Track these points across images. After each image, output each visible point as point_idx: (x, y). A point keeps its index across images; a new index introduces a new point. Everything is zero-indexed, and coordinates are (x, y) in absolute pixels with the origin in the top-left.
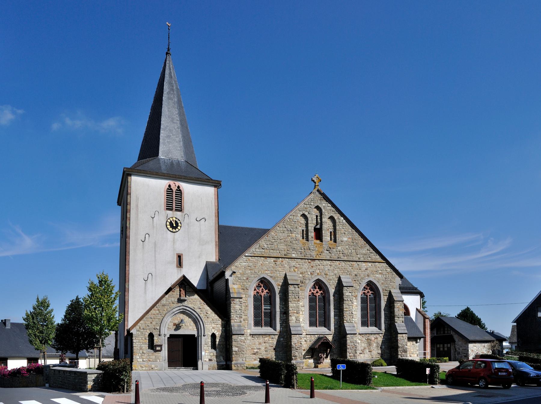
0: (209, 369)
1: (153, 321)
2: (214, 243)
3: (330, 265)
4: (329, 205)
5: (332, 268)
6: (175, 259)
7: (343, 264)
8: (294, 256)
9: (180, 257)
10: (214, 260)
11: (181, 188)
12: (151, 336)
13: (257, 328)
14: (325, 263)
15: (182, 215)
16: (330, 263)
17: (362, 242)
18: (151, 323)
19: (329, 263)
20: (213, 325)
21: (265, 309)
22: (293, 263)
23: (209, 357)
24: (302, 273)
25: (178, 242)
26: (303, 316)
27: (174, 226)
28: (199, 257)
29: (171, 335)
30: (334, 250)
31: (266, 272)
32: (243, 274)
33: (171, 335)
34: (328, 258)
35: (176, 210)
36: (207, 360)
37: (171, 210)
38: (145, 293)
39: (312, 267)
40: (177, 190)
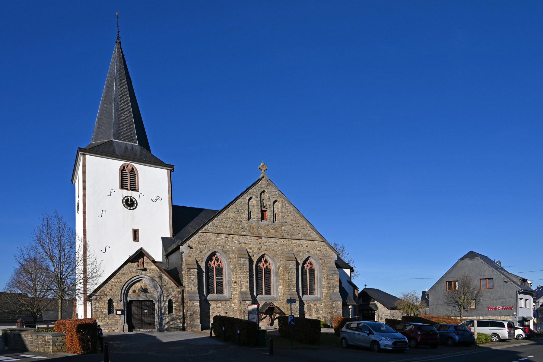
7: (286, 241)
8: (242, 233)
10: (169, 237)
14: (270, 240)
17: (302, 223)
19: (273, 240)
22: (242, 239)
27: (130, 203)
34: (274, 236)
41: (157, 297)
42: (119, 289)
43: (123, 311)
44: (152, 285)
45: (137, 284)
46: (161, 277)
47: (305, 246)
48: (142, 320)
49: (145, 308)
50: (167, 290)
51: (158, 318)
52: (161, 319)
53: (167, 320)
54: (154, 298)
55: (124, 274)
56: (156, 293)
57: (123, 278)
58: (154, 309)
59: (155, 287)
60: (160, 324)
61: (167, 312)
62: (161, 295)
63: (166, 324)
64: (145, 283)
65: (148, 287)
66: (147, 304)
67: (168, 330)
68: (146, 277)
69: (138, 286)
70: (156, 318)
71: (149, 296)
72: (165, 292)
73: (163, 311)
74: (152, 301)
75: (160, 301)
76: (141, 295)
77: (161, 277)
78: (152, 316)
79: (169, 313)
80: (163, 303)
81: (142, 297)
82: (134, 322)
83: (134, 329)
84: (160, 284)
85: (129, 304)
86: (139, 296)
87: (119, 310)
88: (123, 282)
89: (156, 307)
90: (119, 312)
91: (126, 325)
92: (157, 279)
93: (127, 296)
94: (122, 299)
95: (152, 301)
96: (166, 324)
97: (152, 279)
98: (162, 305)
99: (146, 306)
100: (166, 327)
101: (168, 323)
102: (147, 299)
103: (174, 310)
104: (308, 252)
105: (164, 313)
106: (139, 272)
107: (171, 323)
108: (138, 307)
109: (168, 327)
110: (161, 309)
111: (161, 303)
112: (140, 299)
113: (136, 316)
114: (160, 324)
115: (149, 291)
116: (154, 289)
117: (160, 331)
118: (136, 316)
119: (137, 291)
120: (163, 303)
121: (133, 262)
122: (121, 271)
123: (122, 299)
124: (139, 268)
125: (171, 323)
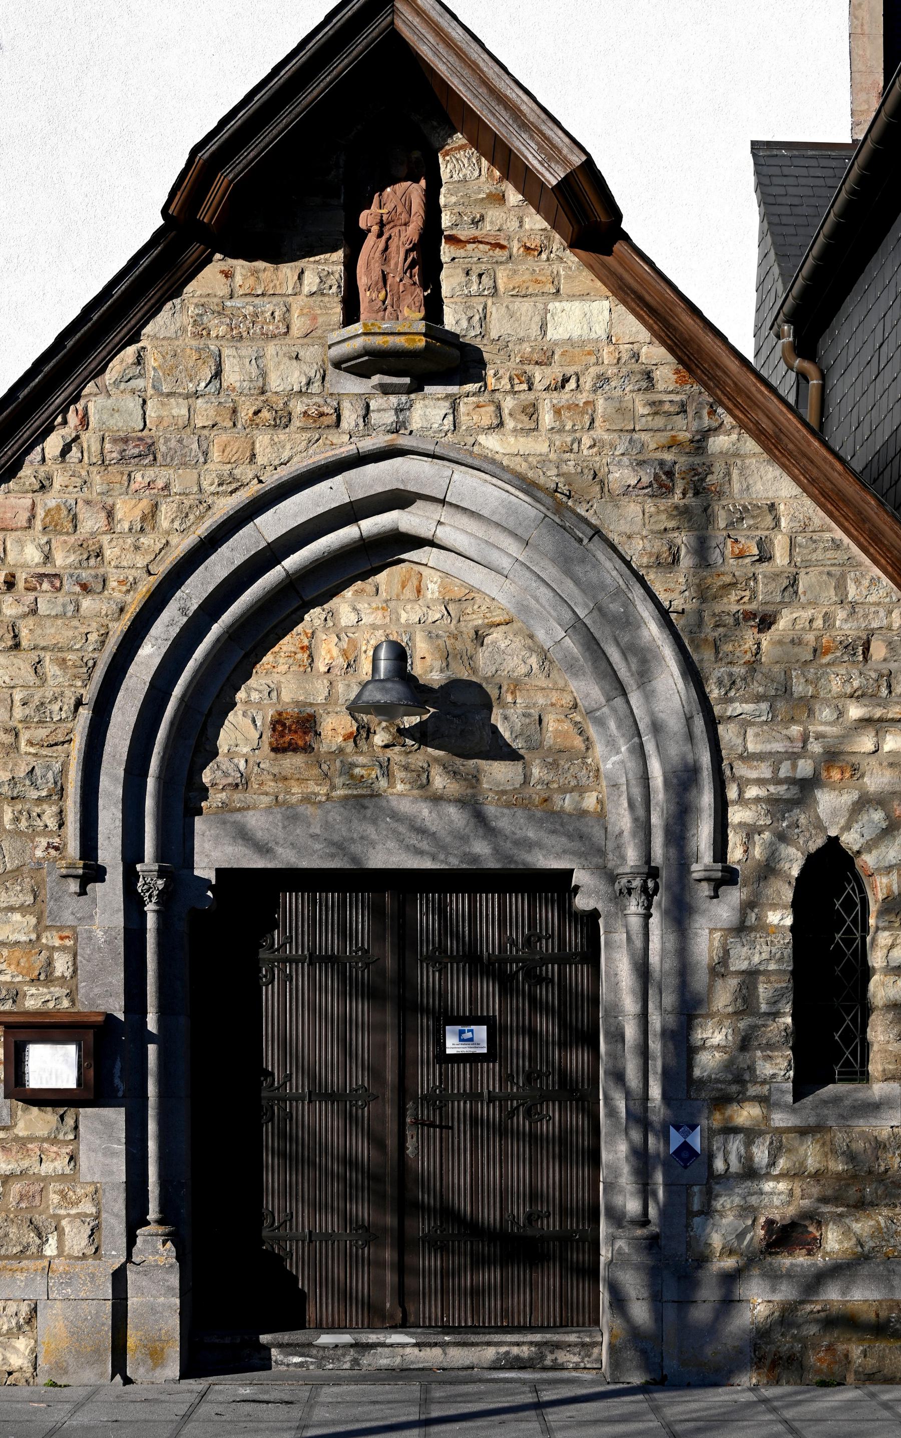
41: (622, 820)
42: (68, 686)
43: (110, 1057)
44: (551, 632)
45: (346, 606)
46: (690, 488)
48: (399, 1188)
49: (459, 988)
50: (786, 700)
51: (642, 1160)
52: (688, 1180)
53: (778, 1197)
54: (592, 844)
55: (141, 450)
56: (612, 759)
57: (128, 511)
58: (582, 1022)
59: (600, 644)
60: (673, 1259)
61: (776, 1067)
62: (683, 781)
63: (753, 1261)
64: (457, 601)
65: (504, 657)
66: (490, 939)
67: (776, 1354)
68: (467, 485)
69: (352, 628)
70: (616, 1153)
71: (516, 799)
72: (752, 737)
73: (714, 1038)
74: (559, 884)
75: (670, 888)
76: (398, 791)
77: (690, 488)
78: (554, 1118)
79: (806, 1081)
80: (724, 910)
81: (416, 820)
82: (297, 1214)
83: (291, 1314)
84: (674, 590)
85: (211, 942)
86: (364, 800)
87: (50, 1029)
88: (131, 569)
89: (618, 969)
90: (53, 1066)
91: (157, 1252)
92: (636, 524)
93: (184, 799)
94: (110, 852)
95: (559, 884)
96: (753, 1261)
97: (564, 517)
98: (705, 943)
99: (474, 962)
100: (759, 1302)
101: (786, 1235)
102: (482, 851)
103: (880, 1034)
105: (736, 1082)
106: (367, 409)
107: (834, 1241)
108: (350, 987)
109: (786, 1317)
110: (689, 1010)
111: (681, 915)
112: (386, 856)
113: (323, 1120)
114: (673, 1259)
115: (506, 723)
116: (588, 690)
117: (660, 1381)
118: (323, 1120)
119: (335, 727)
120: (724, 910)
121: (277, 257)
122: (107, 404)
123: (110, 852)
124: (354, 340)
125: (834, 1241)
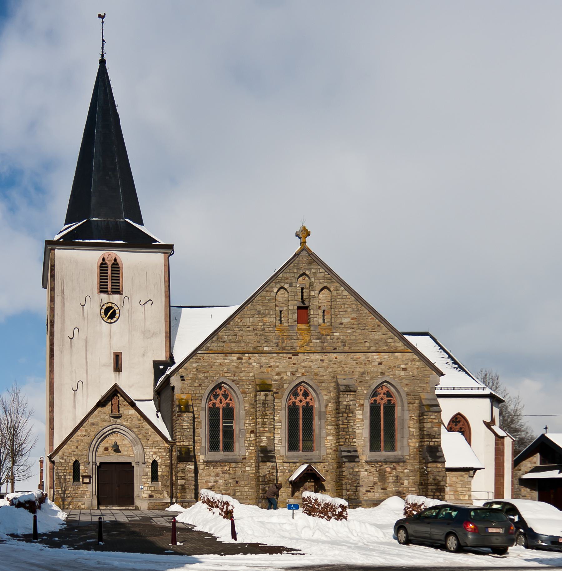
0: (149, 508)
1: (79, 445)
2: (164, 334)
3: (322, 360)
4: (322, 270)
5: (324, 364)
6: (112, 361)
8: (266, 349)
9: (117, 357)
11: (118, 261)
12: (76, 465)
13: (213, 453)
15: (121, 299)
16: (321, 358)
18: (77, 447)
20: (154, 450)
21: (225, 427)
23: (150, 492)
24: (278, 374)
25: (116, 335)
26: (279, 436)
28: (144, 355)
29: (101, 463)
30: (328, 338)
31: (226, 375)
32: (193, 379)
33: (101, 463)
35: (113, 292)
36: (146, 496)
37: (106, 292)
38: (74, 407)
39: (294, 364)
40: (113, 264)
47: (377, 363)
104: (383, 373)
